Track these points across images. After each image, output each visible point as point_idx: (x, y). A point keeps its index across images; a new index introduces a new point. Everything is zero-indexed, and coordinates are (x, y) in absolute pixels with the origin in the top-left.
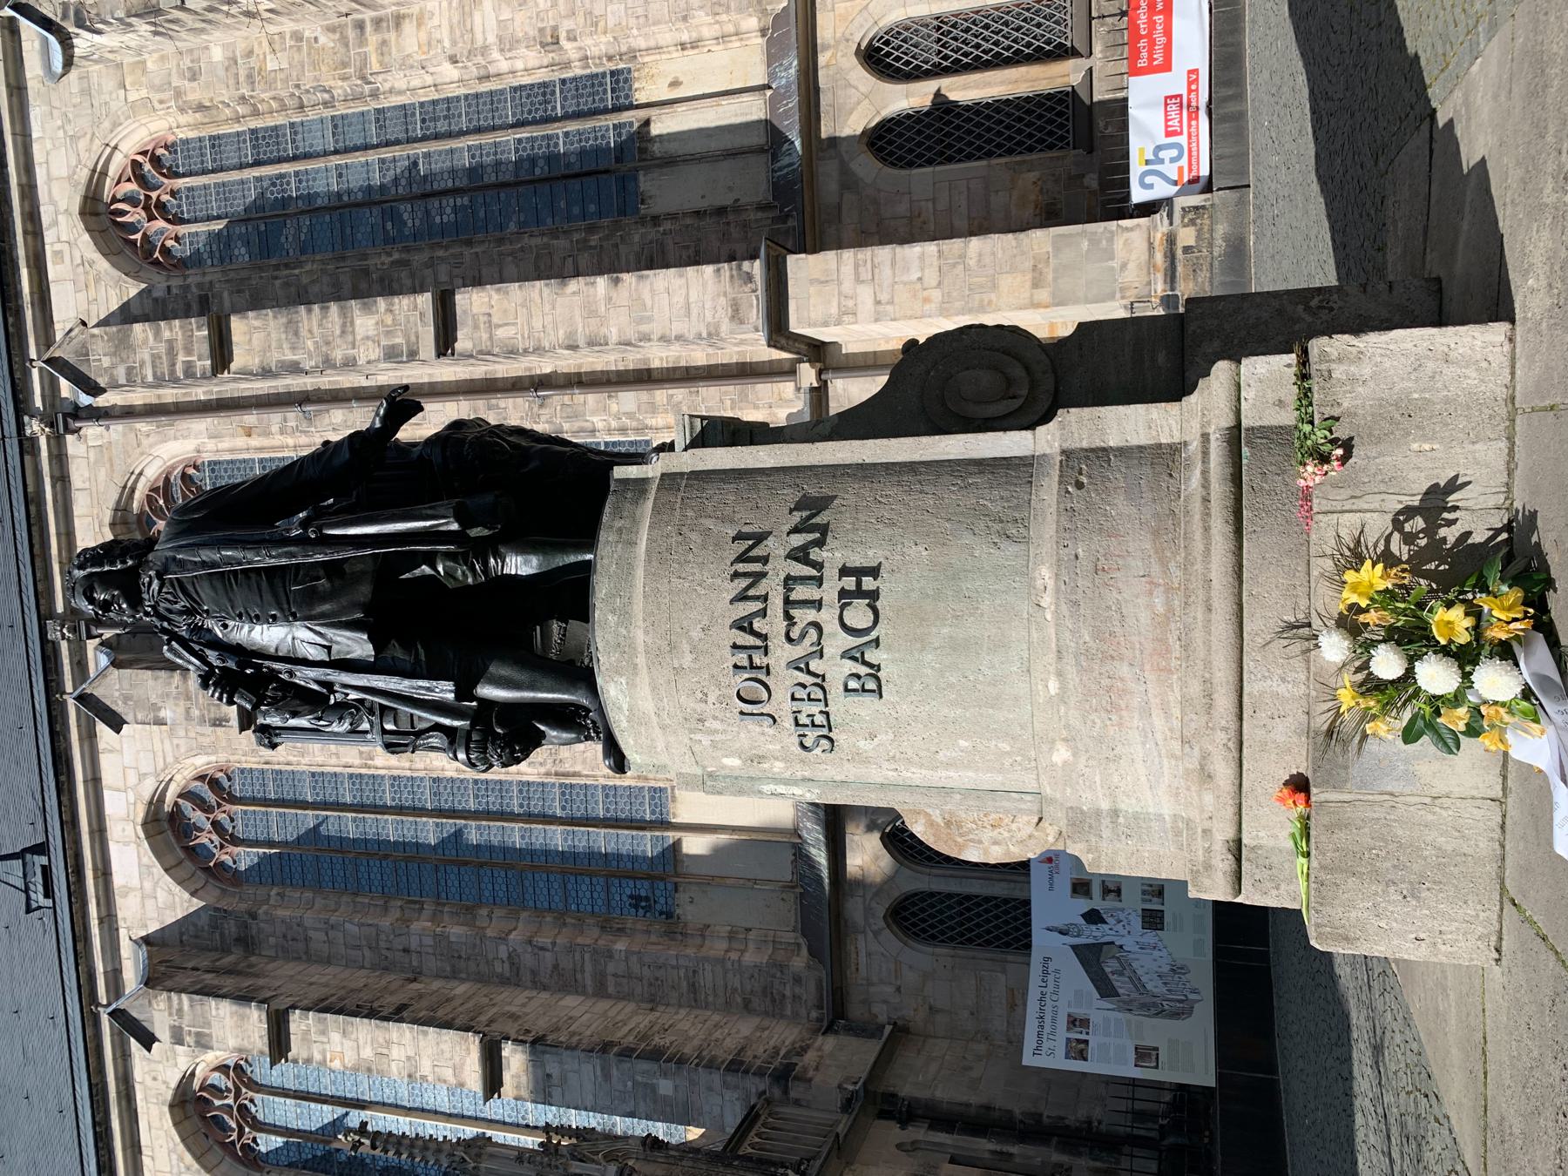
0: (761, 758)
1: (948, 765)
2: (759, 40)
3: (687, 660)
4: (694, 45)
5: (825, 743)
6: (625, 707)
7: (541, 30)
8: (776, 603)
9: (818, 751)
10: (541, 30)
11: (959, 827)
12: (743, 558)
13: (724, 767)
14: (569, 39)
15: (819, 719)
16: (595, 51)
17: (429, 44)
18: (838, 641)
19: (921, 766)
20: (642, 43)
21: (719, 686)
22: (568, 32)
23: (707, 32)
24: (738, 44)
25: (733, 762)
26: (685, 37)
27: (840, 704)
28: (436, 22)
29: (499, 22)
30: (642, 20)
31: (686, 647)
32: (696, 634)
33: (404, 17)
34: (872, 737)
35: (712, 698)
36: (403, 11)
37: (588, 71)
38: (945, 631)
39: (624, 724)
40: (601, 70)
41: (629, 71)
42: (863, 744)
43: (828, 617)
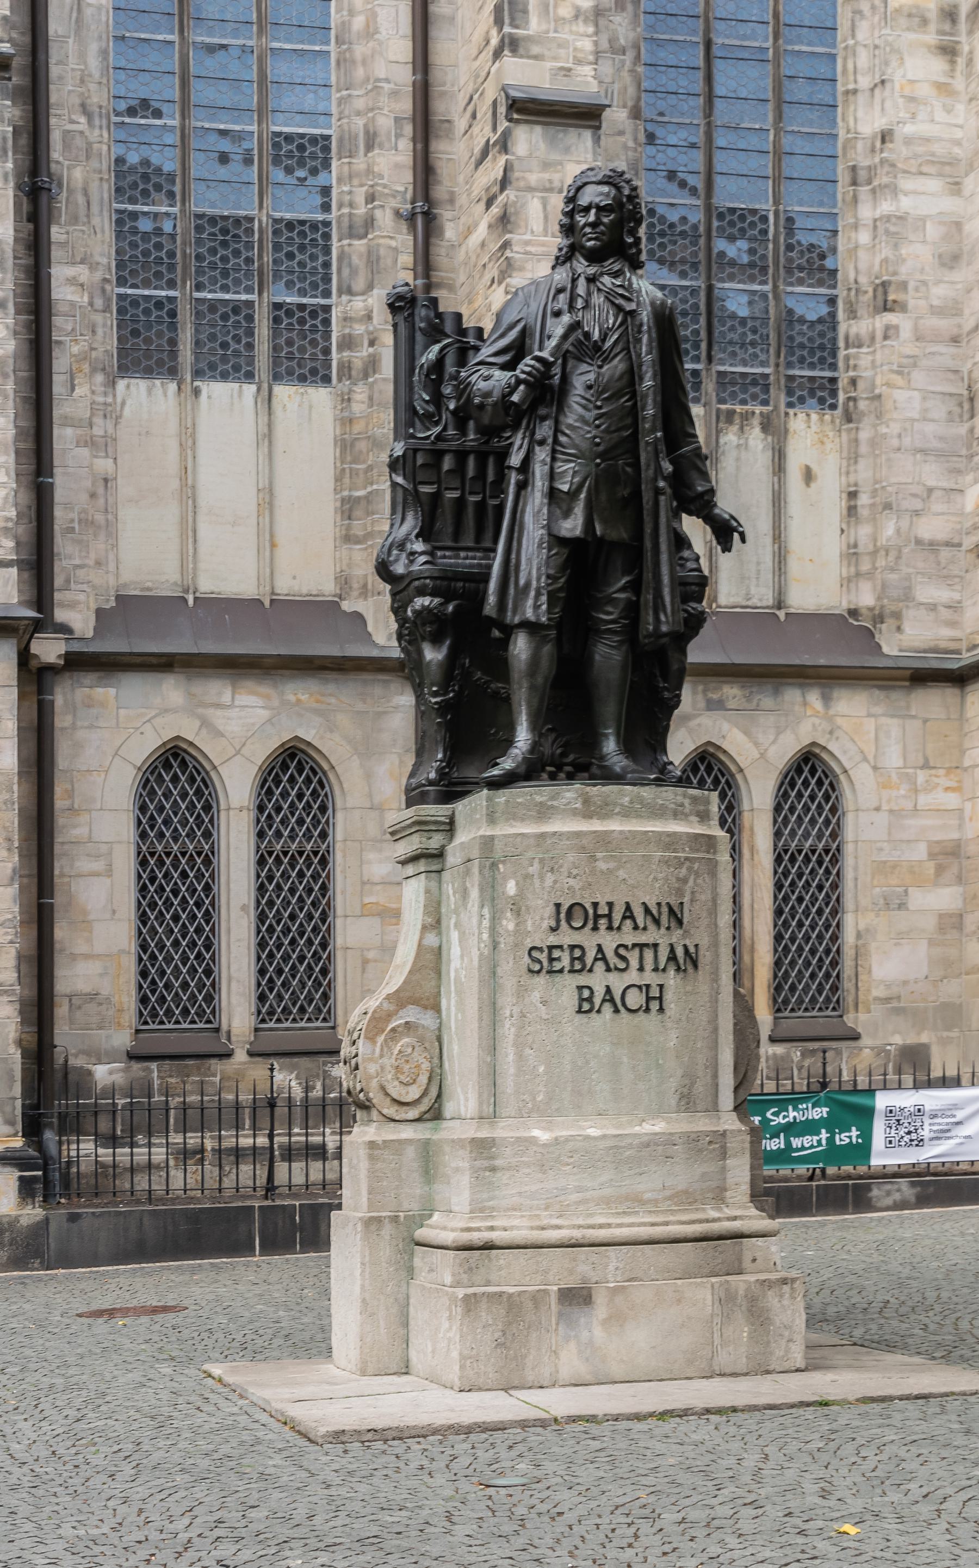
0: (518, 913)
1: (520, 1056)
2: (845, 605)
3: (602, 865)
4: (852, 511)
5: (537, 967)
6: (555, 803)
7: (904, 286)
8: (643, 938)
9: (527, 959)
10: (904, 286)
11: (392, 1039)
12: (671, 911)
13: (505, 879)
14: (887, 328)
15: (557, 966)
16: (865, 361)
17: (912, 99)
18: (618, 983)
19: (517, 1036)
20: (864, 435)
21: (582, 889)
22: (896, 328)
23: (863, 532)
24: (845, 574)
25: (511, 888)
26: (864, 499)
27: (570, 982)
28: (940, 116)
29: (923, 219)
30: (895, 442)
31: (612, 865)
32: (622, 874)
33: (953, 62)
34: (544, 1003)
35: (572, 882)
36: (961, 61)
37: (841, 344)
38: (625, 1059)
39: (538, 799)
40: (841, 364)
41: (833, 407)
42: (536, 996)
43: (632, 976)
